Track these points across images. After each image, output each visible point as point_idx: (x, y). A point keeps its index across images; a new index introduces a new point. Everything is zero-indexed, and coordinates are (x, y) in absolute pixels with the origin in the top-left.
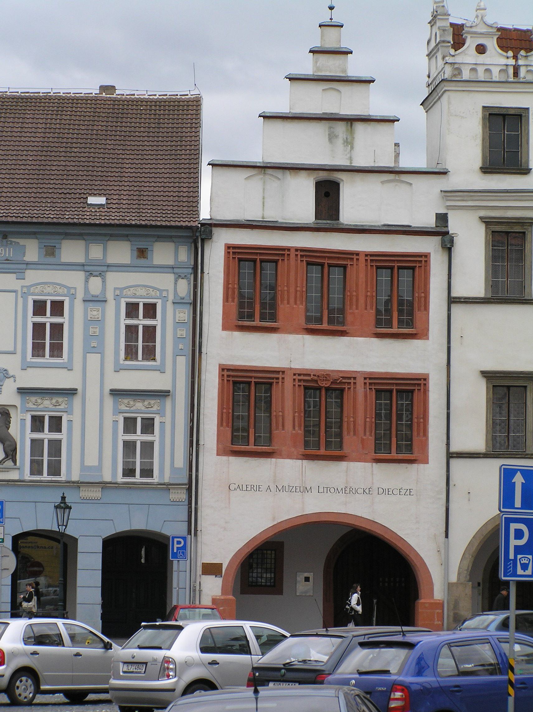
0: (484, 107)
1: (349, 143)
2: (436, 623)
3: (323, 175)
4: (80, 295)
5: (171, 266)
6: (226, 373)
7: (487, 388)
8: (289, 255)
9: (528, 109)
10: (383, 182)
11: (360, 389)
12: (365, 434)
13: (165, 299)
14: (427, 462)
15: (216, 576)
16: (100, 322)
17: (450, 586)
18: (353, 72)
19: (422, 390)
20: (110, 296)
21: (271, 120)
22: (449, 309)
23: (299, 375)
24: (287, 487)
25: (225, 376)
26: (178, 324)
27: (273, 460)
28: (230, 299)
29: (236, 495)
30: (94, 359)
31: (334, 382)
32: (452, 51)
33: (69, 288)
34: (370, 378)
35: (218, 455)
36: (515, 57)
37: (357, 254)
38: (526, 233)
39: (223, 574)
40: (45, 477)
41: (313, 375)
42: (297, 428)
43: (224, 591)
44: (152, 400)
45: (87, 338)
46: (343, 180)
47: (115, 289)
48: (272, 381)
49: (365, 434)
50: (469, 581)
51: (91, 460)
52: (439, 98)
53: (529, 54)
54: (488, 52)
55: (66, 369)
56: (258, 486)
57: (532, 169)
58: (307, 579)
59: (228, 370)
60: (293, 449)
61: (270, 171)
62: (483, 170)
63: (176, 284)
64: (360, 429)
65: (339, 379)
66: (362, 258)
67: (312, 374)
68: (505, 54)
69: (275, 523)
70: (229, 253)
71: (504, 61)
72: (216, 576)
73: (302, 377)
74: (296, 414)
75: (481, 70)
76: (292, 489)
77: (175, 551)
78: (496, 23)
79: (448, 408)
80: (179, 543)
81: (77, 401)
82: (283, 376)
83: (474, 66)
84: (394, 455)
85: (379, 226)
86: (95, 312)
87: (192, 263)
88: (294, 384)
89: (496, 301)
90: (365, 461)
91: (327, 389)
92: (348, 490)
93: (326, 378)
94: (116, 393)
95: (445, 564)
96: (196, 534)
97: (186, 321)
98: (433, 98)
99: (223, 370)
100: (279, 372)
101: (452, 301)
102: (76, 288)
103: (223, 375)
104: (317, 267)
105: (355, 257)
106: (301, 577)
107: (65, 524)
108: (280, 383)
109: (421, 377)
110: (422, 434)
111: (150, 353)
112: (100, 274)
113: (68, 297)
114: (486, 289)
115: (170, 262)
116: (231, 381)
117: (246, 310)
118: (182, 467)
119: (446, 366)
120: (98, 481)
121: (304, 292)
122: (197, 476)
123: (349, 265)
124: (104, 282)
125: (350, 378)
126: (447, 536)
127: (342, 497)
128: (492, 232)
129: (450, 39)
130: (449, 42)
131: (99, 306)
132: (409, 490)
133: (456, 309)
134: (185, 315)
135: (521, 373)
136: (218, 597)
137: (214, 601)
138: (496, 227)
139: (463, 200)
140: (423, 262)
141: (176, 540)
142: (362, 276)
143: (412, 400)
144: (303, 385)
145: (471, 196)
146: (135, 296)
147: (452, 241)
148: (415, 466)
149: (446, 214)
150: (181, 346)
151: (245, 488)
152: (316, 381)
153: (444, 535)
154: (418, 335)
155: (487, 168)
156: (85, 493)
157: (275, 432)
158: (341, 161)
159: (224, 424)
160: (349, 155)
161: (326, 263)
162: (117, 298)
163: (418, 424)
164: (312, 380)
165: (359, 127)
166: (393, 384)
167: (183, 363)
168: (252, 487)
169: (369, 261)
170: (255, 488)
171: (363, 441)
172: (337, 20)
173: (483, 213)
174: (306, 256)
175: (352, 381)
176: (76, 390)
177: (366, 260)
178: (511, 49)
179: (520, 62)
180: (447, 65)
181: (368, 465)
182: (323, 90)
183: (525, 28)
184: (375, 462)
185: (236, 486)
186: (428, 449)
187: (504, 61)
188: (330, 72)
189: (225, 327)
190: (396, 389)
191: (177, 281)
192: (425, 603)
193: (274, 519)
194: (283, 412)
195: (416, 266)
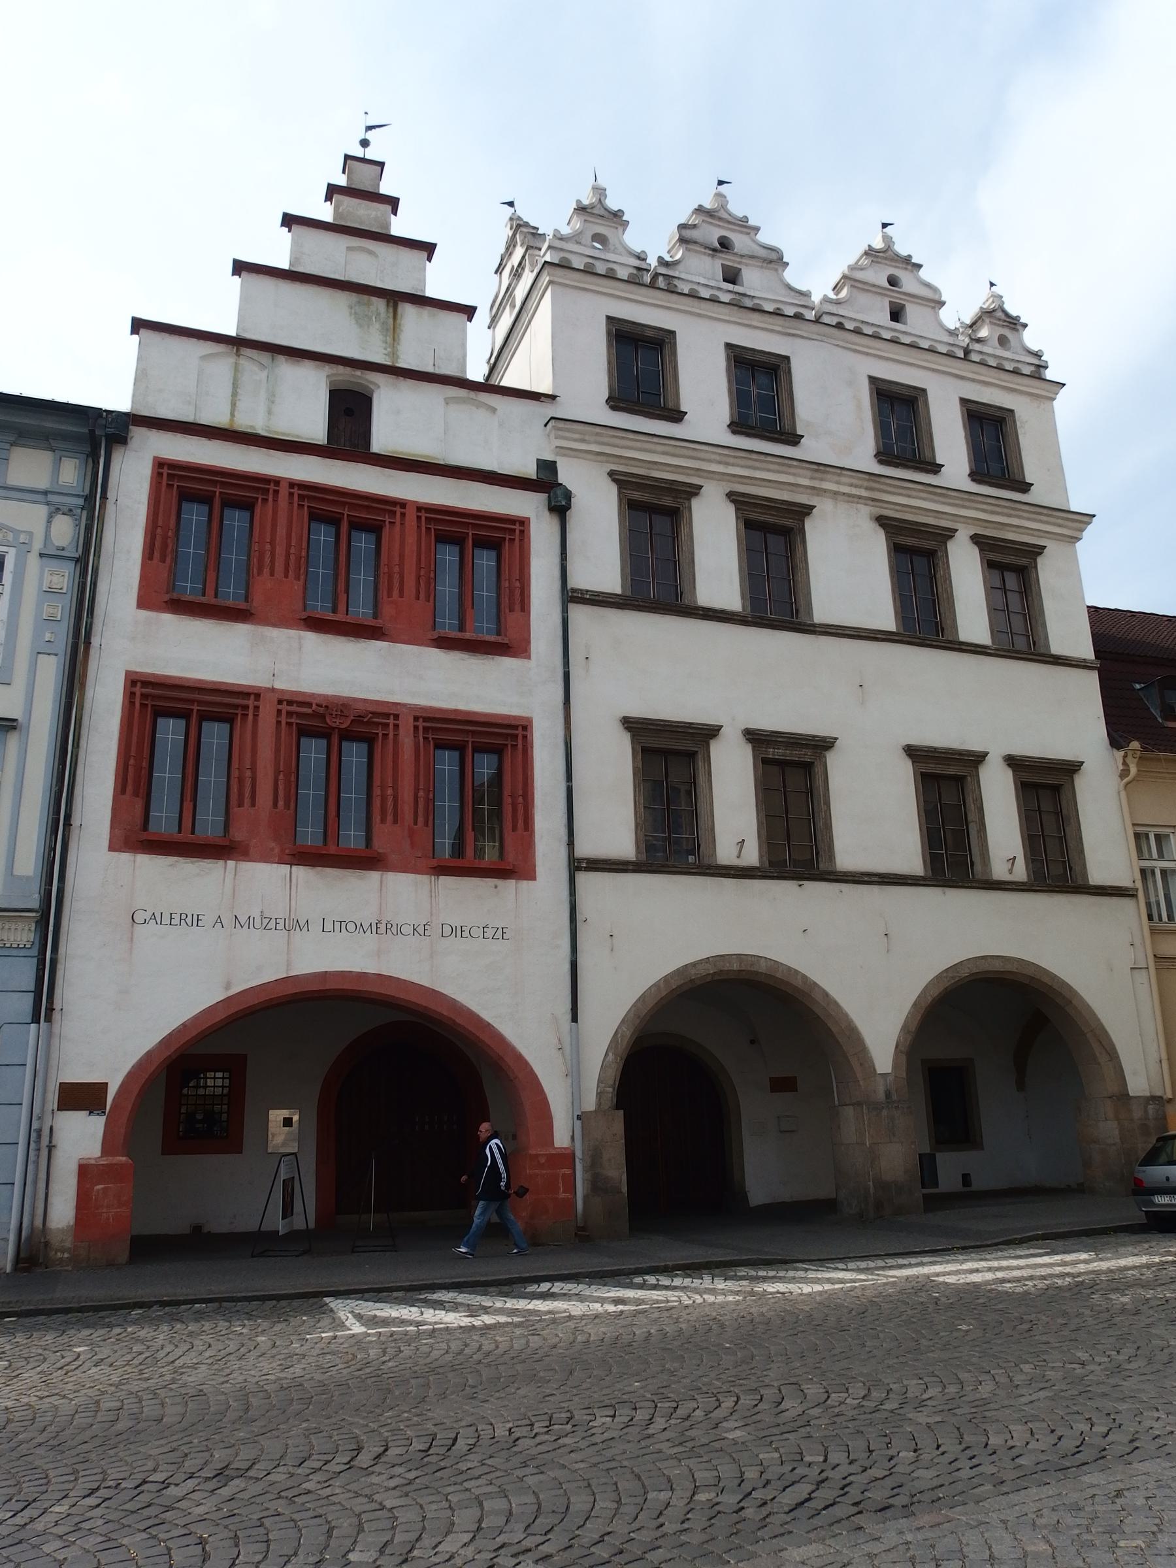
1: (393, 332)
2: (562, 1195)
8: (276, 492)
10: (447, 401)
13: (24, 549)
19: (520, 746)
22: (565, 611)
23: (290, 703)
24: (258, 921)
27: (231, 863)
28: (157, 555)
29: (147, 933)
31: (359, 719)
34: (425, 719)
35: (112, 848)
37: (403, 504)
38: (681, 509)
39: (108, 1107)
41: (317, 705)
42: (281, 803)
46: (379, 387)
49: (416, 823)
50: (618, 1107)
60: (273, 844)
63: (49, 522)
64: (407, 810)
70: (160, 474)
73: (294, 708)
74: (281, 776)
76: (269, 923)
87: (87, 491)
90: (415, 871)
95: (574, 1073)
96: (49, 1019)
97: (64, 591)
98: (508, 350)
100: (249, 694)
101: (571, 597)
103: (133, 694)
105: (398, 509)
108: (251, 717)
115: (43, 484)
116: (149, 706)
117: (189, 585)
121: (303, 559)
122: (61, 891)
123: (387, 523)
125: (387, 716)
126: (575, 1019)
127: (370, 941)
132: (500, 930)
133: (578, 613)
134: (63, 577)
136: (93, 1162)
142: (411, 540)
143: (500, 768)
144: (297, 723)
148: (511, 884)
149: (555, 462)
150: (48, 636)
151: (166, 920)
152: (323, 717)
153: (569, 1017)
154: (511, 650)
157: (235, 810)
159: (130, 788)
163: (514, 806)
164: (315, 715)
165: (409, 312)
166: (468, 731)
167: (50, 672)
168: (183, 918)
169: (423, 519)
170: (189, 920)
171: (412, 834)
174: (309, 498)
177: (419, 518)
181: (424, 879)
185: (148, 915)
186: (535, 852)
191: (52, 517)
192: (537, 1156)
193: (228, 986)
194: (253, 769)
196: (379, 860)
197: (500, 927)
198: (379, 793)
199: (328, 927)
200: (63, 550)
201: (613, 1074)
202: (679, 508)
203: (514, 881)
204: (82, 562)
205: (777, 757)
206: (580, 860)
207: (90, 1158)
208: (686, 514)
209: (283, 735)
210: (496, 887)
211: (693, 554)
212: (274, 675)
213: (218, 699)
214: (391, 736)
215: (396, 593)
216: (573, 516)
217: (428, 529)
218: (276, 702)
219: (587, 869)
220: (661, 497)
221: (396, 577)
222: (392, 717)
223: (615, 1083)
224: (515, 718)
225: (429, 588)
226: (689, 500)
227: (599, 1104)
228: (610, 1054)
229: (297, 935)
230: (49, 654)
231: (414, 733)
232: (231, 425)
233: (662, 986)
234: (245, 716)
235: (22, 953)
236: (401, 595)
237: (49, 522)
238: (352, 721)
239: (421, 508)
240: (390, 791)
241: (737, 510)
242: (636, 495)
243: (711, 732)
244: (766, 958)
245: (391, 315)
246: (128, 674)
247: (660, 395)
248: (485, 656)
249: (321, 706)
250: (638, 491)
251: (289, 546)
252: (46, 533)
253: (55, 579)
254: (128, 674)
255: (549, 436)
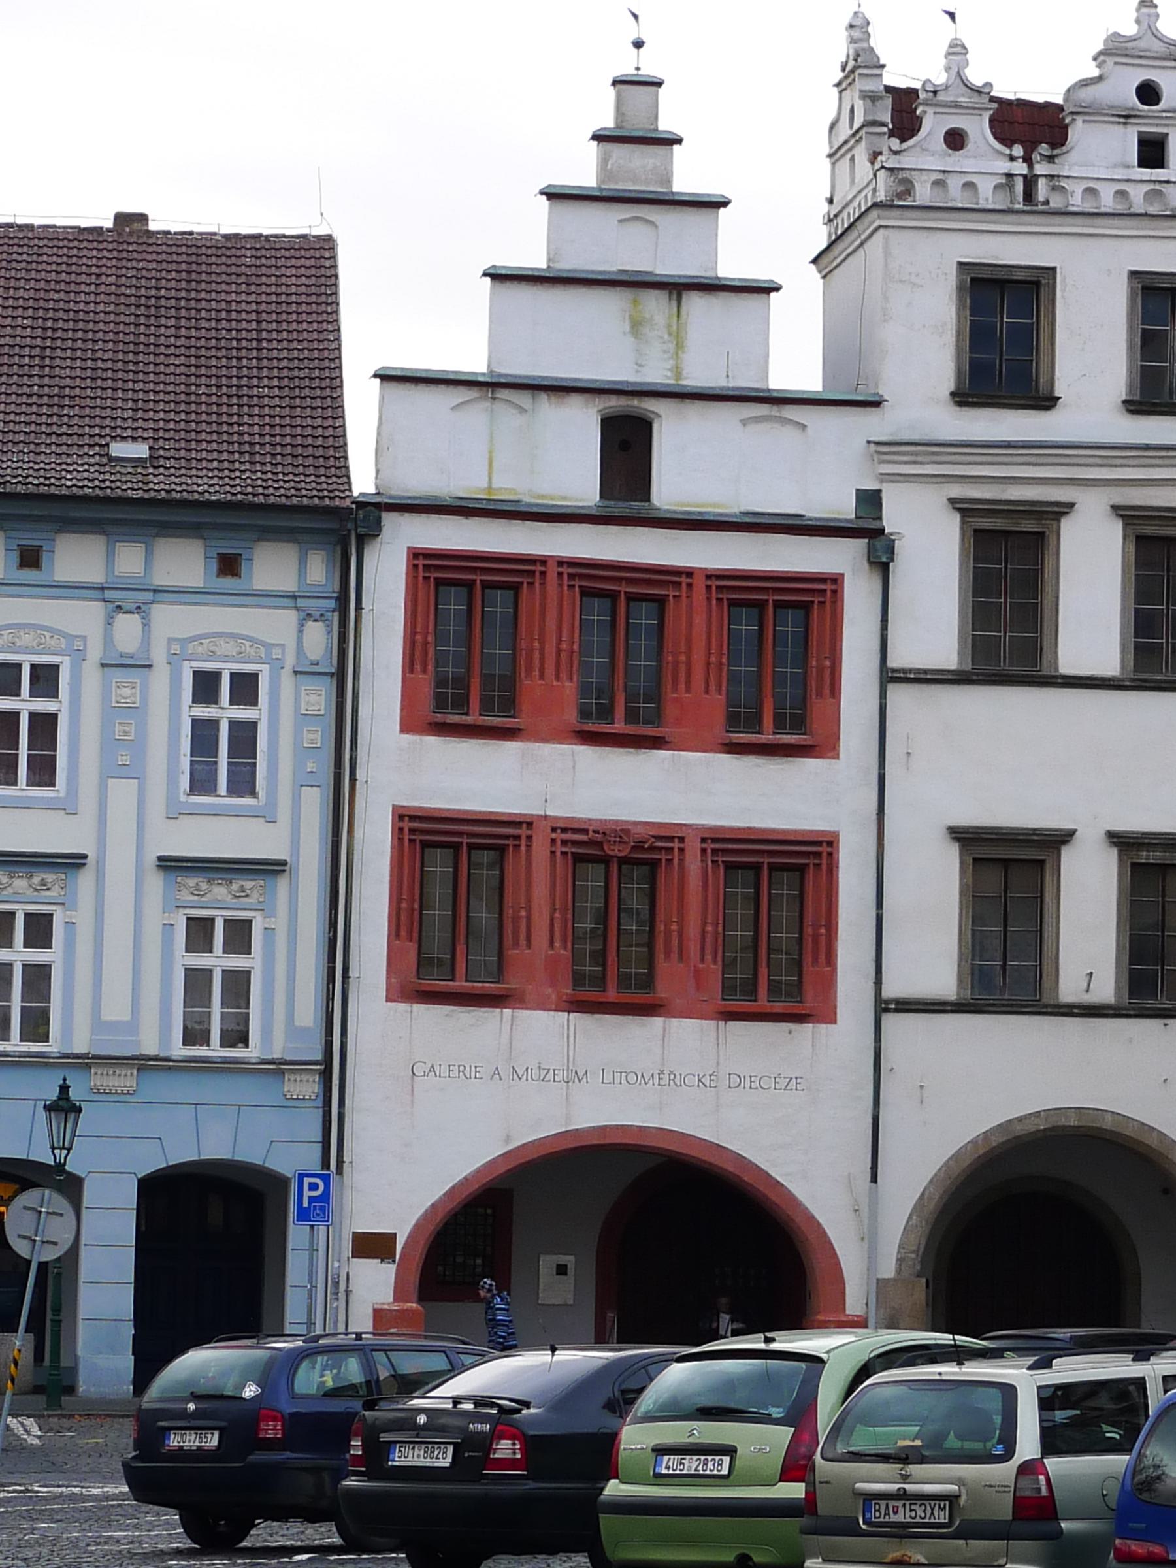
0: (961, 264)
3: (615, 403)
4: (95, 653)
5: (291, 594)
6: (407, 825)
7: (962, 863)
8: (543, 573)
9: (1054, 269)
10: (744, 422)
11: (693, 864)
12: (702, 960)
13: (277, 665)
14: (834, 1021)
15: (382, 1261)
16: (138, 711)
17: (882, 1284)
18: (684, 183)
19: (824, 867)
20: (159, 655)
21: (508, 284)
22: (883, 695)
23: (564, 830)
25: (406, 830)
26: (304, 718)
27: (507, 1012)
28: (418, 667)
30: (122, 792)
31: (638, 847)
32: (895, 143)
33: (71, 638)
34: (714, 840)
35: (388, 1000)
36: (1027, 159)
37: (689, 573)
38: (1047, 533)
40: (215, 1050)
42: (557, 945)
43: (400, 1293)
44: (251, 880)
45: (108, 744)
46: (659, 416)
47: (170, 640)
48: (506, 842)
49: (702, 960)
51: (116, 1009)
52: (862, 244)
53: (1055, 152)
54: (970, 146)
55: (262, 820)
56: (473, 1069)
57: (1059, 398)
58: (562, 1270)
59: (412, 818)
60: (550, 990)
61: (503, 394)
62: (958, 399)
63: (300, 631)
64: (693, 948)
65: (649, 840)
66: (700, 583)
67: (591, 828)
68: (1008, 151)
69: (510, 1147)
70: (416, 566)
71: (1004, 166)
72: (382, 1261)
74: (557, 915)
75: (955, 183)
76: (544, 1075)
77: (305, 1204)
78: (989, 85)
79: (879, 904)
80: (313, 1187)
81: (85, 880)
82: (529, 832)
83: (940, 176)
84: (763, 1002)
85: (735, 516)
86: (126, 690)
87: (337, 587)
88: (553, 849)
89: (981, 678)
91: (623, 861)
92: (665, 1077)
93: (621, 837)
94: (170, 865)
95: (870, 1239)
97: (322, 712)
99: (401, 817)
100: (520, 823)
101: (890, 677)
102: (283, 645)
103: (401, 830)
104: (650, 604)
105: (684, 580)
106: (547, 1263)
107: (66, 1145)
108: (523, 848)
109: (820, 839)
110: (822, 958)
111: (243, 783)
112: (139, 608)
113: (267, 666)
114: (961, 653)
118: (311, 1024)
119: (874, 817)
120: (129, 1054)
123: (671, 598)
124: (146, 625)
125: (671, 839)
126: (874, 1179)
128: (976, 531)
129: (887, 118)
130: (884, 125)
131: (135, 676)
133: (898, 694)
134: (319, 697)
135: (1034, 831)
136: (386, 1307)
137: (379, 1315)
138: (985, 520)
139: (915, 463)
140: (829, 593)
141: (307, 1180)
142: (699, 621)
144: (572, 853)
145: (933, 453)
146: (212, 656)
147: (891, 550)
148: (808, 1027)
149: (879, 491)
150: (310, 767)
152: (599, 845)
154: (817, 749)
155: (968, 395)
156: (100, 1078)
157: (512, 953)
158: (656, 374)
159: (403, 933)
160: (672, 362)
161: (622, 593)
162: (174, 660)
165: (695, 303)
166: (763, 852)
171: (698, 974)
172: (649, 70)
173: (957, 491)
174: (582, 576)
175: (676, 845)
176: (85, 857)
177: (708, 587)
178: (1022, 143)
179: (1041, 169)
180: (883, 170)
181: (711, 1024)
182: (620, 221)
183: (1040, 99)
184: (722, 1020)
187: (1004, 166)
188: (635, 181)
189: (407, 727)
190: (769, 863)
191: (303, 625)
194: (529, 909)
195: (813, 602)
196: (661, 1006)
197: (794, 1076)
198: (662, 928)
199: (608, 1078)
200: (317, 664)
201: (918, 1240)
202: (1044, 533)
203: (811, 1025)
204: (340, 676)
205: (1152, 861)
206: (887, 1002)
207: (383, 1304)
208: (1052, 540)
209: (558, 865)
210: (790, 1032)
211: (1057, 598)
212: (546, 801)
213: (491, 841)
214: (676, 861)
215: (682, 686)
216: (898, 570)
217: (719, 600)
218: (549, 830)
219: (896, 1011)
220: (1020, 521)
221: (683, 668)
222: (676, 840)
223: (919, 1248)
224: (818, 832)
225: (720, 676)
226: (1059, 521)
227: (899, 1270)
228: (914, 1217)
229: (575, 1086)
230: (312, 786)
231: (702, 856)
232: (490, 488)
233: (980, 1142)
234: (517, 847)
235: (308, 1104)
236: (688, 690)
237: (300, 631)
238: (633, 847)
239: (710, 575)
240: (674, 927)
241: (1125, 525)
242: (986, 523)
243: (1060, 839)
244: (1113, 1112)
245: (675, 310)
246: (395, 808)
247: (1032, 361)
248: (785, 759)
249: (598, 832)
250: (988, 518)
251: (560, 641)
252: (298, 644)
253: (313, 698)
254: (395, 808)
255: (872, 456)
